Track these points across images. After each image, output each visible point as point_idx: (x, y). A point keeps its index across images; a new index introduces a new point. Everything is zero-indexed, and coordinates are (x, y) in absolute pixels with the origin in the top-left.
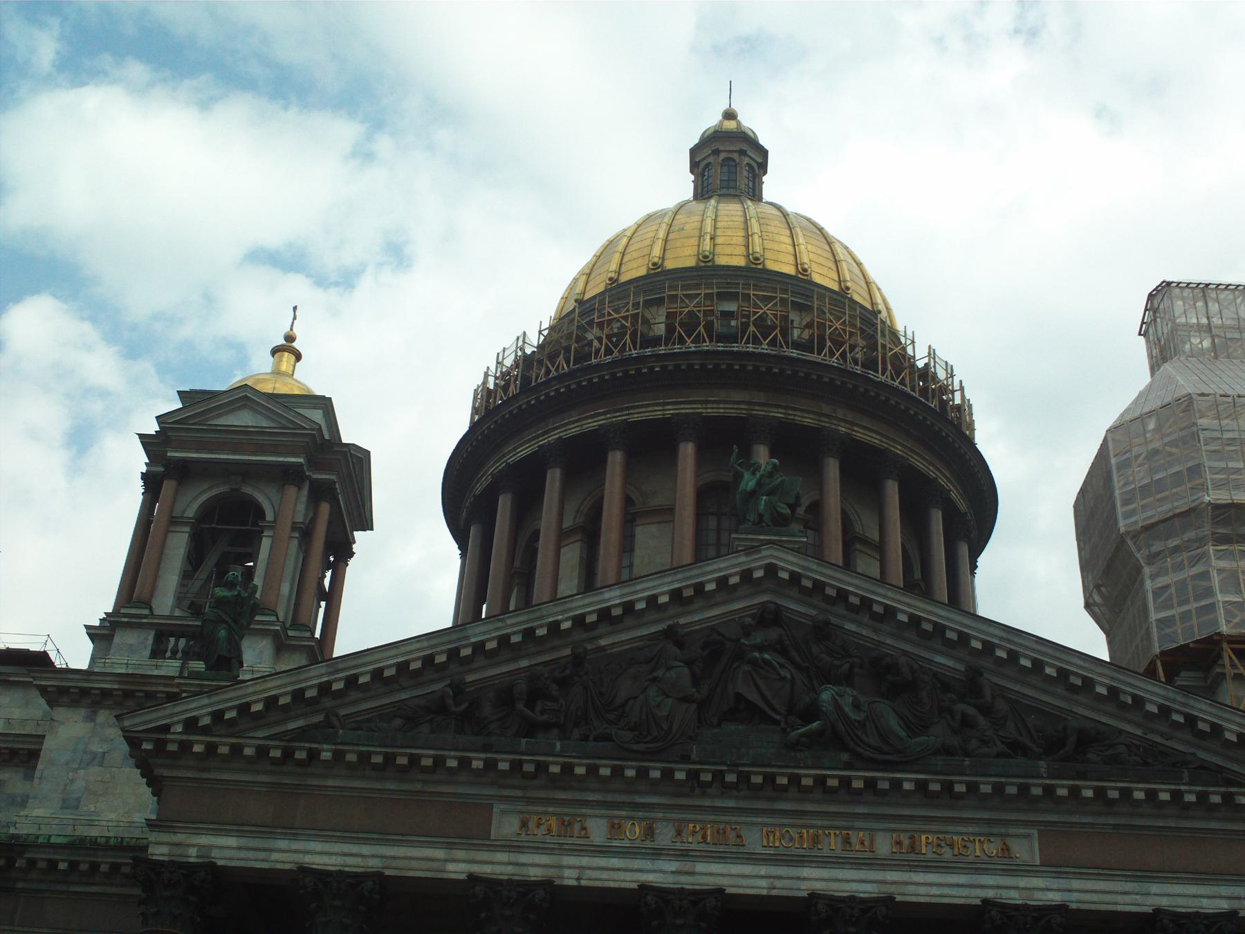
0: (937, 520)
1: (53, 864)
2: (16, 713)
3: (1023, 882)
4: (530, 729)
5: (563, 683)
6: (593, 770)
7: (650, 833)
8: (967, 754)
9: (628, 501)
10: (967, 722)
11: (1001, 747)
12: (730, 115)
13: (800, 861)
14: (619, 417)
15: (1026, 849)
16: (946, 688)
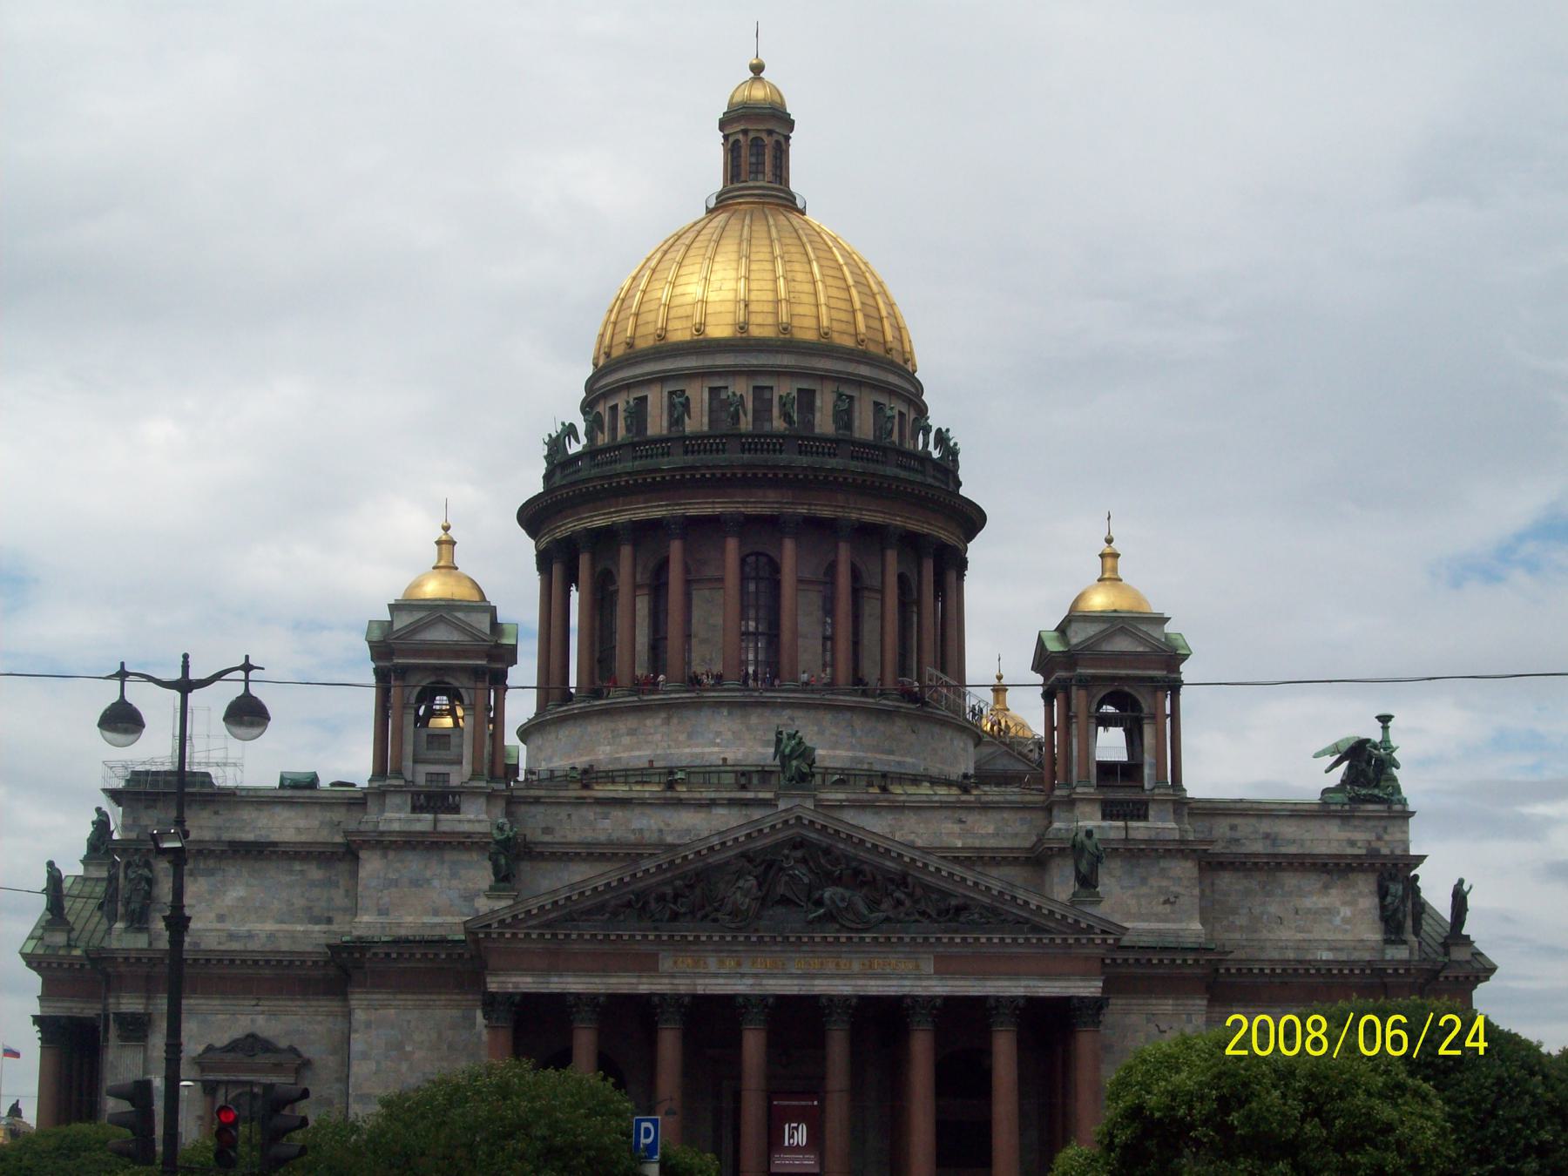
0: (928, 567)
1: (388, 955)
2: (302, 823)
3: (925, 983)
4: (675, 916)
5: (690, 887)
6: (710, 937)
7: (739, 964)
8: (899, 921)
9: (687, 570)
10: (899, 903)
11: (917, 917)
12: (757, 69)
13: (813, 976)
14: (679, 511)
15: (928, 966)
16: (892, 880)
